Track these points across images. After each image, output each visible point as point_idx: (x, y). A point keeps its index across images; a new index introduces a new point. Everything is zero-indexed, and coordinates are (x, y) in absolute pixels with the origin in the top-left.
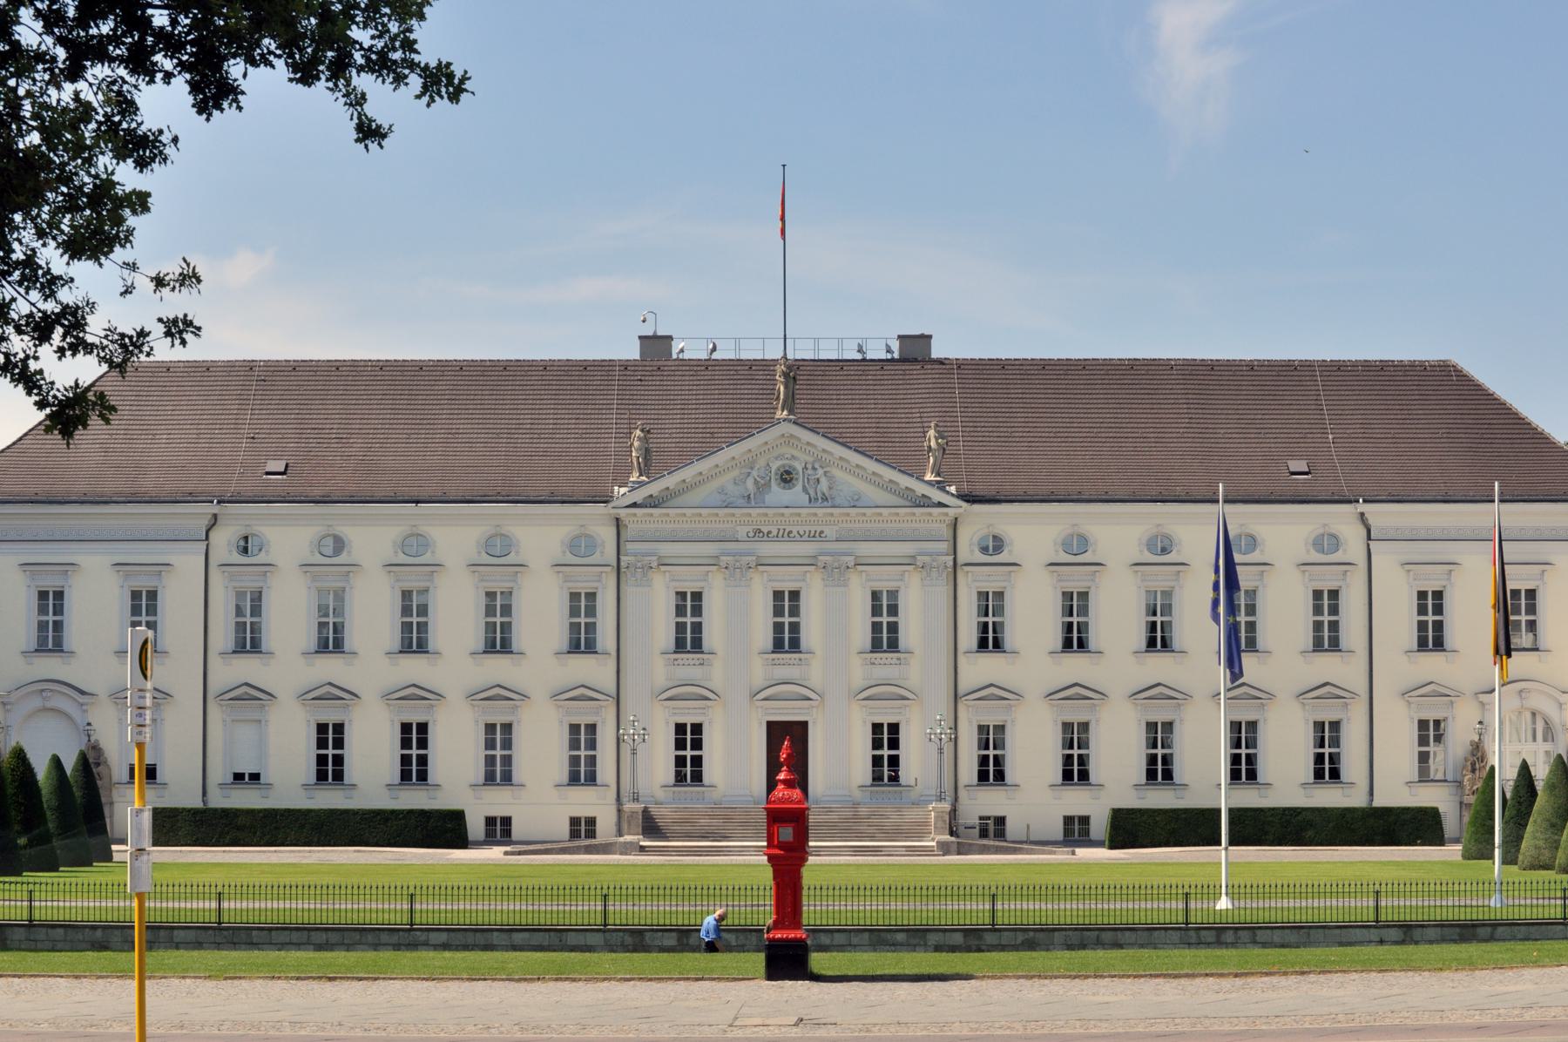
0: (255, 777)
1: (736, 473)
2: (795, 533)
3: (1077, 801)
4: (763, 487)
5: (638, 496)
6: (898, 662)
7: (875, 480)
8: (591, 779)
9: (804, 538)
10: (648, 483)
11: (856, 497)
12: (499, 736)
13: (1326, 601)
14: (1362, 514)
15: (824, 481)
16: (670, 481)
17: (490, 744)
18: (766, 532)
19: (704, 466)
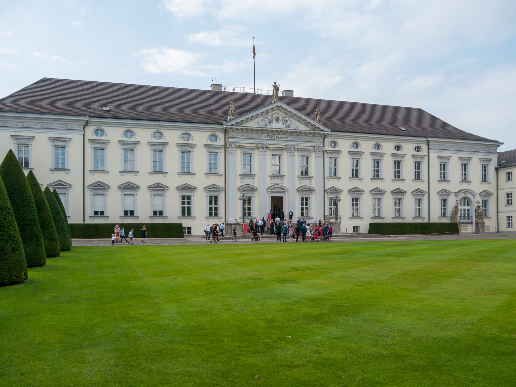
0: (102, 213)
1: (262, 118)
2: (279, 137)
3: (356, 222)
4: (270, 122)
5: (234, 122)
6: (309, 179)
7: (303, 121)
8: (216, 214)
9: (282, 139)
10: (235, 119)
11: (297, 127)
12: (186, 201)
13: (418, 165)
14: (428, 141)
15: (289, 122)
16: (244, 118)
17: (183, 203)
18: (271, 136)
19: (254, 114)
